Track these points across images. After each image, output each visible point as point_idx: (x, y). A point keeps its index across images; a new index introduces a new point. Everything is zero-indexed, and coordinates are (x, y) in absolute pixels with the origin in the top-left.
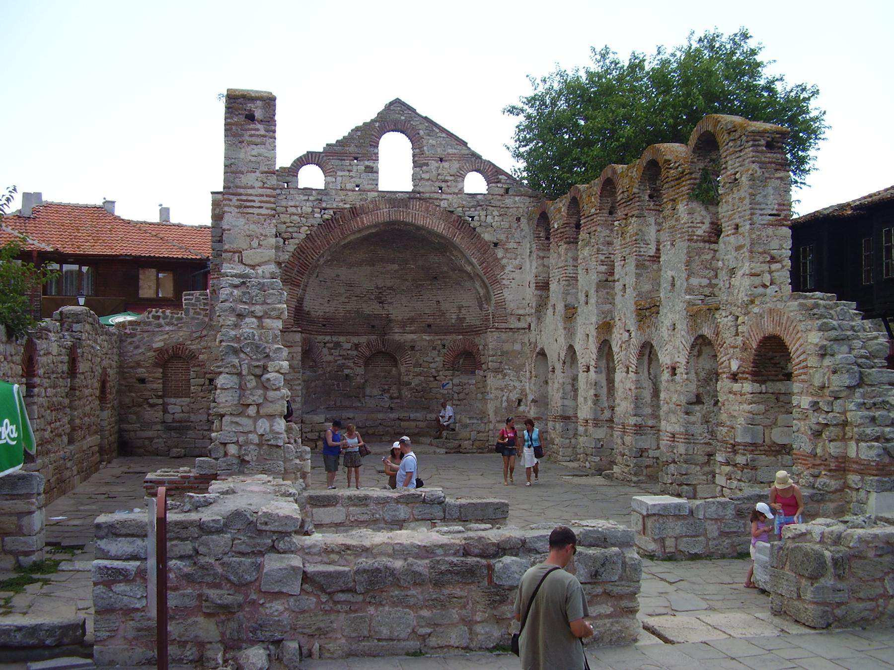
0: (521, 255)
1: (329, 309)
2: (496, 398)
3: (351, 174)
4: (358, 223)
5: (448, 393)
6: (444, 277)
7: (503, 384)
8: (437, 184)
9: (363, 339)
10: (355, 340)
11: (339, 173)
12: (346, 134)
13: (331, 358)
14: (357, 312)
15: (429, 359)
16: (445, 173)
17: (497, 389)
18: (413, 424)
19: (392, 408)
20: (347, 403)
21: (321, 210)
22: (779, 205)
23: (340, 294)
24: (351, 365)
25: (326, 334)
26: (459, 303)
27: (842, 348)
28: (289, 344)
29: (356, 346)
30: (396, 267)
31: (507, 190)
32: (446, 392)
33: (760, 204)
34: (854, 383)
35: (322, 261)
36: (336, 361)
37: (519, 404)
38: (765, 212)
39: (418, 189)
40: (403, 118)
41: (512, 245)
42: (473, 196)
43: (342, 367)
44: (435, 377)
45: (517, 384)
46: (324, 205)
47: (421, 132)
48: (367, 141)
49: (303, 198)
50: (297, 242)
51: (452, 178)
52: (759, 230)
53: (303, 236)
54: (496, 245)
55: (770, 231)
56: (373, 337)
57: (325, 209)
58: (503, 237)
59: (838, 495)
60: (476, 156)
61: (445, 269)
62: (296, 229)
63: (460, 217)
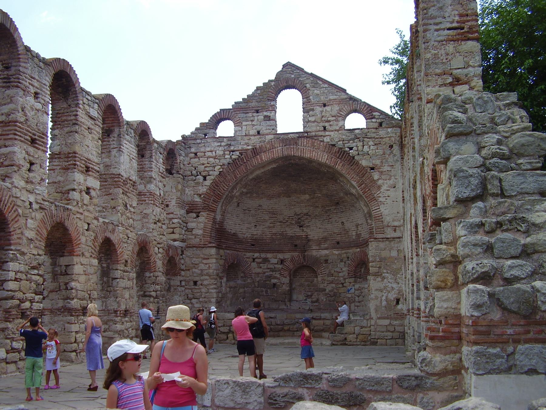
0: (395, 176)
1: (257, 232)
2: (376, 298)
3: (253, 123)
4: (258, 160)
5: (352, 297)
6: (343, 202)
7: (381, 285)
8: (322, 124)
9: (287, 256)
10: (281, 256)
11: (244, 123)
12: (251, 93)
13: (259, 270)
14: (282, 234)
15: (338, 269)
16: (328, 115)
17: (377, 290)
18: (321, 322)
19: (311, 311)
20: (274, 306)
21: (230, 152)
22: (461, 15)
23: (265, 221)
24: (278, 276)
25: (254, 251)
26: (354, 222)
27: (463, 148)
28: (206, 257)
29: (282, 261)
30: (307, 197)
31: (381, 124)
32: (350, 296)
33: (435, 18)
34: (467, 193)
35: (236, 193)
36: (264, 273)
37: (398, 303)
38: (442, 26)
39: (309, 130)
40: (293, 76)
41: (386, 168)
42: (351, 131)
43: (270, 277)
44: (343, 284)
45: (395, 285)
46: (232, 148)
47: (308, 86)
48: (265, 96)
49: (217, 144)
50: (212, 177)
51: (334, 118)
52: (435, 48)
53: (217, 173)
54: (372, 169)
55: (450, 47)
56: (296, 254)
57: (233, 151)
58: (378, 162)
59: (449, 380)
60: (352, 99)
61: (342, 195)
62: (211, 168)
63: (341, 148)
